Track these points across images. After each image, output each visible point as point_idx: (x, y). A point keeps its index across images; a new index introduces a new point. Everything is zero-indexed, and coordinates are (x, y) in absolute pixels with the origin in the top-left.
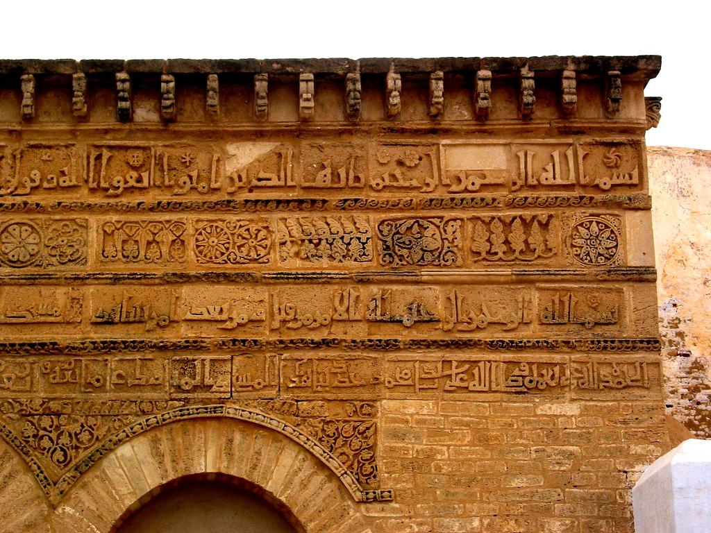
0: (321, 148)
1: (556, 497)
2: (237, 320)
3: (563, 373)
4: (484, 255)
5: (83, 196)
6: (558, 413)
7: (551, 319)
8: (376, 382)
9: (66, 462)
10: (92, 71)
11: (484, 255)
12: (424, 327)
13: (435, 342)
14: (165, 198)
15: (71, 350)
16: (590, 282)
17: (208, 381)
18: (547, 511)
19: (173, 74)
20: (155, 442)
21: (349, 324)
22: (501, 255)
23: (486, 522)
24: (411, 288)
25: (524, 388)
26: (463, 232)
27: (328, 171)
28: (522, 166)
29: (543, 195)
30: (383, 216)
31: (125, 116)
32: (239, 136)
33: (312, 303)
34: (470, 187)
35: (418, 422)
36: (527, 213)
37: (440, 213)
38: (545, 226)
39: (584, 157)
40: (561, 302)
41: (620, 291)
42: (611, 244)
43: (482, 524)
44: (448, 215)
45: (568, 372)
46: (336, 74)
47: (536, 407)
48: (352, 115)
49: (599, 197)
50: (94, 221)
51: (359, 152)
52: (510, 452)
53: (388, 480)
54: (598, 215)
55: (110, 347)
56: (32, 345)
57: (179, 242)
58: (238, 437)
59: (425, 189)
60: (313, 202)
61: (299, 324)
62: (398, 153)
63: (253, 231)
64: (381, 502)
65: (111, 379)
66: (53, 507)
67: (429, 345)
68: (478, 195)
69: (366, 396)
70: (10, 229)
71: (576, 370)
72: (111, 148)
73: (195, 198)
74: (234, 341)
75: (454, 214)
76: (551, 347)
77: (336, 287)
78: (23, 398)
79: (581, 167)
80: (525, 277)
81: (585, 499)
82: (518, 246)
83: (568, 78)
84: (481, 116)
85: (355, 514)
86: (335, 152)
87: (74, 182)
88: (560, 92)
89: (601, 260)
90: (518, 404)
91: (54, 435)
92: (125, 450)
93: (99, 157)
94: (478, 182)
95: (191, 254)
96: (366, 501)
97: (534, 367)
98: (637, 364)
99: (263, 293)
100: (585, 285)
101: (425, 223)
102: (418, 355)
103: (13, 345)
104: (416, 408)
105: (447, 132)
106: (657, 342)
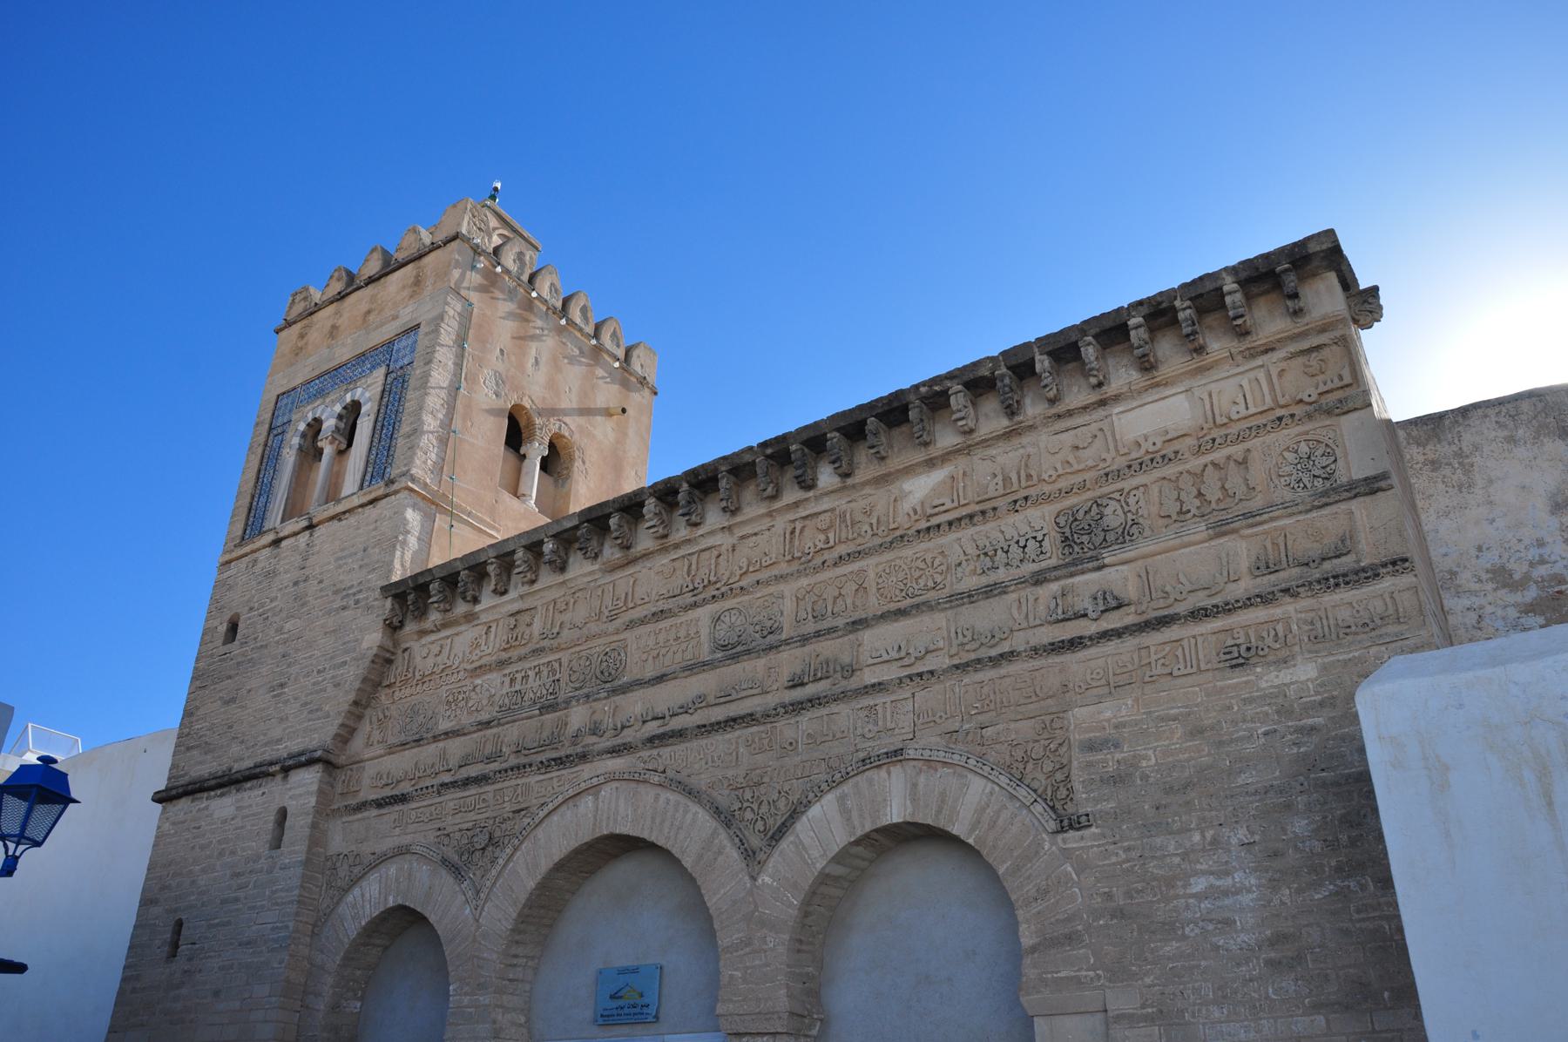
0: (992, 458)
1: (1299, 788)
2: (914, 654)
4: (1174, 517)
5: (784, 568)
6: (1287, 681)
7: (1264, 567)
9: (765, 832)
10: (769, 451)
11: (1174, 517)
13: (1126, 628)
14: (851, 548)
17: (889, 725)
18: (1288, 806)
19: (838, 430)
20: (842, 799)
21: (1030, 632)
23: (1209, 834)
25: (1238, 659)
27: (1000, 477)
28: (1208, 407)
29: (1234, 429)
30: (1057, 507)
31: (807, 484)
32: (909, 471)
33: (986, 616)
35: (1116, 727)
36: (1218, 455)
37: (1119, 485)
38: (1243, 463)
39: (1281, 373)
43: (1204, 836)
44: (1126, 485)
45: (1295, 627)
46: (983, 378)
47: (1259, 677)
48: (1011, 411)
50: (787, 589)
51: (1031, 450)
52: (1232, 741)
53: (1084, 801)
55: (797, 707)
56: (734, 720)
57: (861, 588)
59: (1102, 465)
60: (983, 513)
61: (974, 645)
63: (929, 561)
64: (1078, 829)
66: (754, 878)
67: (1118, 633)
71: (1305, 622)
73: (877, 541)
74: (910, 677)
76: (1266, 599)
77: (1014, 596)
78: (730, 773)
79: (1277, 387)
80: (1224, 528)
81: (1339, 784)
82: (1213, 494)
83: (1230, 293)
84: (1147, 365)
86: (1007, 457)
88: (1223, 306)
90: (1237, 678)
91: (755, 806)
92: (815, 811)
93: (792, 532)
96: (1062, 830)
98: (1387, 596)
99: (940, 619)
100: (1300, 518)
101: (1105, 502)
102: (1111, 646)
103: (719, 723)
105: (1117, 398)
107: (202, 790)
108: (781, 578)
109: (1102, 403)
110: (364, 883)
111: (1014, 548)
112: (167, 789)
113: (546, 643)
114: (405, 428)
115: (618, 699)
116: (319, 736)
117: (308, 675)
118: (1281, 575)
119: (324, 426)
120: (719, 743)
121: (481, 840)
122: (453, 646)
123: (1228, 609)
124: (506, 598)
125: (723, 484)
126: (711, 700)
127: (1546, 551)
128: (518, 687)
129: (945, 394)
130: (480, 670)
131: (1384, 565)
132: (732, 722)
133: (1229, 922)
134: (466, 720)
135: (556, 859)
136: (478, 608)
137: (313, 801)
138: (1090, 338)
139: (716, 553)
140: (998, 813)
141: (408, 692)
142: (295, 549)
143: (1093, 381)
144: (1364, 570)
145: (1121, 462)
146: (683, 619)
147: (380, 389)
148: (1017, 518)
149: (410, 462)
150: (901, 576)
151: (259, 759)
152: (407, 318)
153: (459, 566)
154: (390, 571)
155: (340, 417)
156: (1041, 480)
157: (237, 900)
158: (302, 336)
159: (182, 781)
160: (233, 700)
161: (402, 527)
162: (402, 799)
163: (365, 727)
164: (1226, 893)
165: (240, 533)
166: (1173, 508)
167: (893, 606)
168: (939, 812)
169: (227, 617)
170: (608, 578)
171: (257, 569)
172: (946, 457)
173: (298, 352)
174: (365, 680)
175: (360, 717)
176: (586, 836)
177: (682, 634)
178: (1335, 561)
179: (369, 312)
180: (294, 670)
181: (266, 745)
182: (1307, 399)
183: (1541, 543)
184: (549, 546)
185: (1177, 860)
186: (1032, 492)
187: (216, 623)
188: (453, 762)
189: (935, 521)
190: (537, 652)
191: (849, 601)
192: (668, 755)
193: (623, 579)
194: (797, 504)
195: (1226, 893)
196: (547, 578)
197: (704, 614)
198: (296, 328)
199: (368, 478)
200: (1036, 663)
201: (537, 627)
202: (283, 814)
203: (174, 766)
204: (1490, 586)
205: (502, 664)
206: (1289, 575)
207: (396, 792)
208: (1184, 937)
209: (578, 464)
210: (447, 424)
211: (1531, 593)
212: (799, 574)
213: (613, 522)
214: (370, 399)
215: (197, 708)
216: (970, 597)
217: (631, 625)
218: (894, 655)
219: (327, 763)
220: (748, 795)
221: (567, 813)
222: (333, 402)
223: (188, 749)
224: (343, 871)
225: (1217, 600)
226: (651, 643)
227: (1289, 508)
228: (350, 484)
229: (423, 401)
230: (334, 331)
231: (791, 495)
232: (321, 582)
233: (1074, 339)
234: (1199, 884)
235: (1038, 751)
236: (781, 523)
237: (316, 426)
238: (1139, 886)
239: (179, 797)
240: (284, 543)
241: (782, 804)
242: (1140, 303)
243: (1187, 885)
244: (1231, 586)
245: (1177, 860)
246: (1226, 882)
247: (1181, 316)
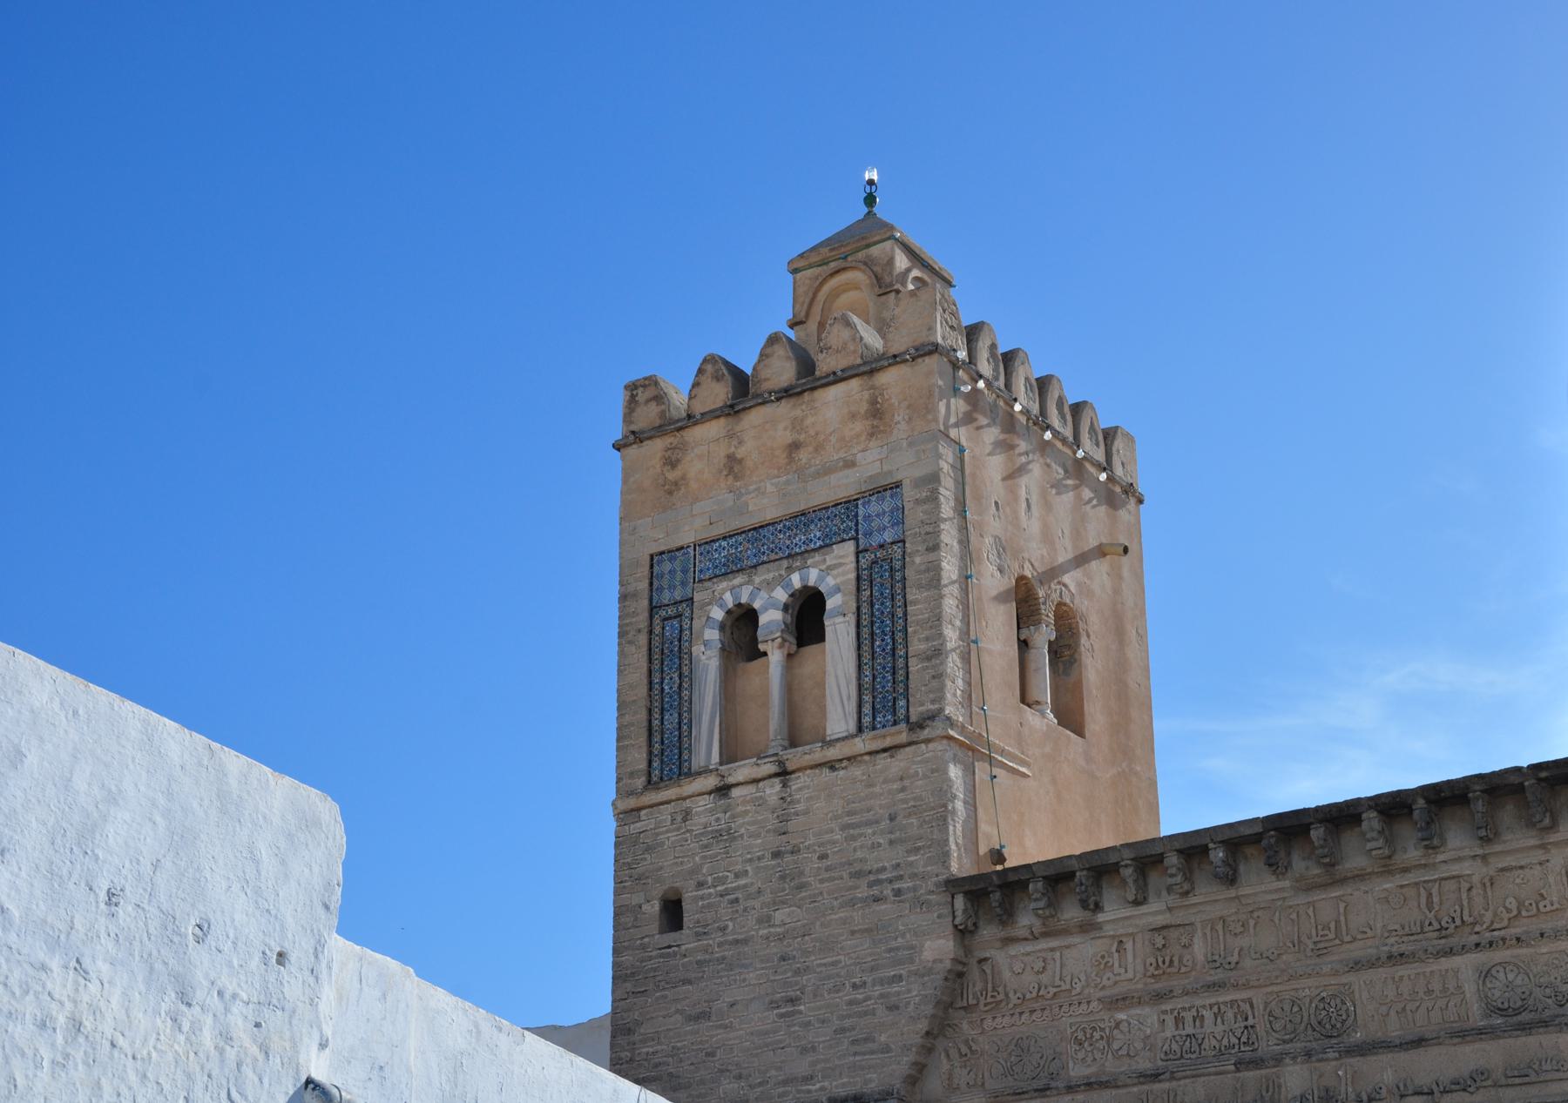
10: (1543, 774)
70: (1493, 972)
87: (1556, 906)
113: (1218, 976)
114: (917, 646)
117: (837, 989)
119: (763, 619)
124: (1144, 909)
128: (1189, 1030)
130: (1115, 1003)
134: (1111, 1066)
136: (1101, 917)
139: (1465, 886)
141: (1007, 1020)
142: (760, 802)
146: (1434, 967)
147: (853, 576)
152: (875, 469)
153: (1075, 865)
155: (786, 608)
160: (703, 1016)
161: (943, 794)
163: (942, 1065)
165: (643, 765)
169: (658, 891)
170: (1302, 899)
171: (696, 824)
173: (672, 488)
175: (929, 1050)
177: (1436, 986)
179: (795, 446)
180: (808, 980)
181: (785, 1082)
187: (636, 899)
193: (1326, 903)
197: (1465, 964)
199: (867, 709)
201: (1199, 950)
209: (1084, 640)
210: (965, 634)
214: (837, 589)
215: (639, 1023)
217: (1356, 966)
222: (770, 585)
226: (1391, 993)
229: (940, 606)
230: (733, 465)
232: (823, 857)
240: (735, 792)
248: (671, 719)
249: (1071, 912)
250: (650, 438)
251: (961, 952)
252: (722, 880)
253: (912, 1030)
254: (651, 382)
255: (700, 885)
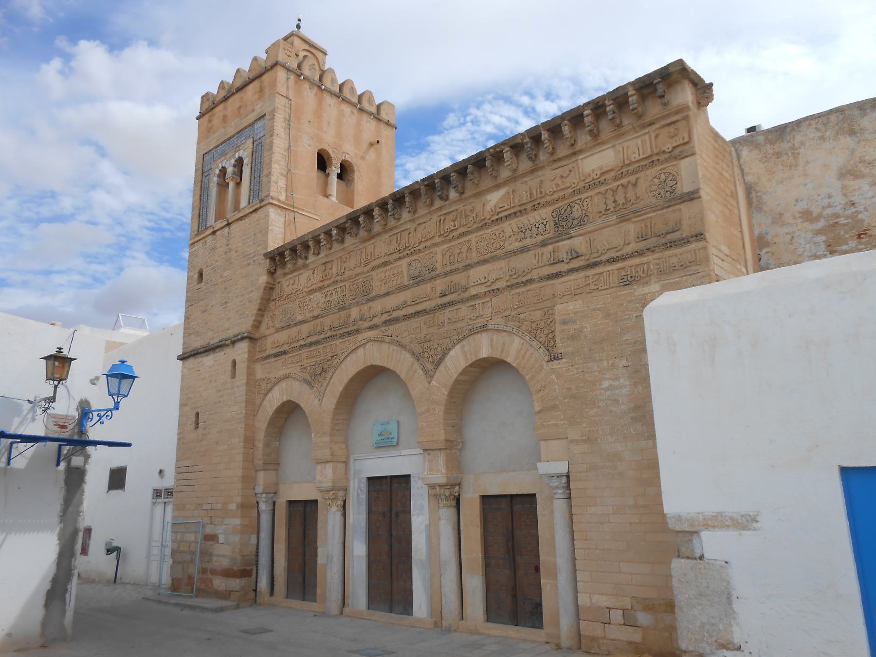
3: (649, 268)
5: (437, 240)
7: (642, 238)
8: (554, 296)
10: (426, 183)
12: (576, 261)
15: (432, 311)
16: (662, 209)
19: (455, 172)
20: (463, 347)
22: (612, 209)
23: (611, 362)
24: (567, 242)
25: (627, 282)
26: (595, 202)
30: (553, 208)
31: (444, 198)
34: (595, 177)
35: (574, 313)
36: (624, 181)
37: (579, 197)
38: (635, 185)
39: (656, 137)
40: (646, 226)
41: (680, 210)
42: (672, 183)
44: (583, 196)
49: (662, 158)
50: (439, 250)
53: (561, 347)
54: (664, 169)
55: (444, 306)
57: (469, 249)
58: (495, 337)
60: (520, 211)
62: (559, 172)
65: (446, 321)
66: (429, 383)
68: (602, 179)
69: (549, 304)
72: (445, 214)
73: (476, 226)
74: (489, 291)
75: (586, 195)
76: (640, 253)
77: (533, 252)
78: (418, 336)
79: (654, 144)
82: (621, 201)
83: (632, 96)
84: (595, 135)
85: (547, 367)
86: (532, 182)
89: (668, 194)
90: (626, 291)
92: (452, 353)
94: (599, 173)
95: (474, 254)
96: (551, 360)
97: (633, 268)
99: (502, 264)
102: (573, 276)
104: (574, 306)
105: (581, 151)
106: (701, 234)
107: (198, 354)
108: (436, 245)
109: (574, 154)
110: (273, 391)
111: (534, 229)
112: (183, 354)
113: (338, 278)
114: (265, 172)
115: (370, 304)
116: (245, 325)
118: (648, 241)
120: (414, 323)
121: (319, 370)
122: (300, 280)
123: (622, 258)
124: (320, 256)
125: (407, 199)
126: (409, 303)
127: (832, 200)
129: (501, 152)
131: (692, 237)
132: (417, 314)
133: (616, 401)
134: (309, 315)
135: (350, 377)
136: (308, 262)
137: (246, 356)
138: (566, 122)
140: (526, 352)
143: (569, 143)
144: (683, 239)
145: (582, 185)
148: (536, 213)
149: (269, 190)
150: (486, 242)
151: (221, 338)
152: (259, 111)
154: (266, 246)
155: (234, 166)
156: (546, 194)
157: (220, 402)
158: (210, 121)
159: (189, 350)
160: (206, 311)
162: (284, 353)
163: (266, 320)
164: (616, 388)
166: (602, 208)
167: (482, 258)
168: (502, 352)
172: (505, 183)
174: (262, 299)
175: (262, 316)
176: (361, 366)
177: (396, 272)
178: (672, 234)
179: (240, 108)
182: (667, 150)
183: (830, 197)
184: (334, 232)
185: (597, 374)
186: (542, 201)
187: (192, 274)
188: (304, 336)
189: (501, 215)
190: (335, 282)
191: (464, 255)
192: (392, 329)
193: (369, 245)
194: (441, 208)
195: (616, 388)
196: (336, 246)
197: (404, 262)
198: (207, 116)
200: (542, 284)
201: (334, 270)
202: (234, 363)
203: (184, 343)
204: (800, 221)
205: (321, 289)
206: (652, 242)
207: (282, 350)
208: (599, 407)
211: (821, 223)
212: (443, 242)
213: (361, 219)
216: (514, 253)
217: (372, 269)
218: (483, 281)
219: (251, 339)
220: (425, 346)
221: (353, 356)
222: (230, 158)
223: (190, 335)
224: (263, 386)
225: (619, 254)
226: (383, 276)
227: (654, 208)
228: (243, 203)
230: (225, 119)
231: (438, 203)
233: (559, 122)
234: (606, 384)
235: (542, 324)
236: (435, 218)
237: (223, 171)
238: (582, 385)
239: (189, 357)
240: (218, 233)
241: (439, 349)
242: (589, 103)
243: (600, 384)
244: (626, 247)
245: (597, 374)
246: (616, 383)
247: (608, 109)
248: (205, 210)
249: (300, 262)
250: (205, 114)
251: (271, 281)
252: (212, 264)
253: (253, 308)
254: (207, 94)
255: (207, 266)
